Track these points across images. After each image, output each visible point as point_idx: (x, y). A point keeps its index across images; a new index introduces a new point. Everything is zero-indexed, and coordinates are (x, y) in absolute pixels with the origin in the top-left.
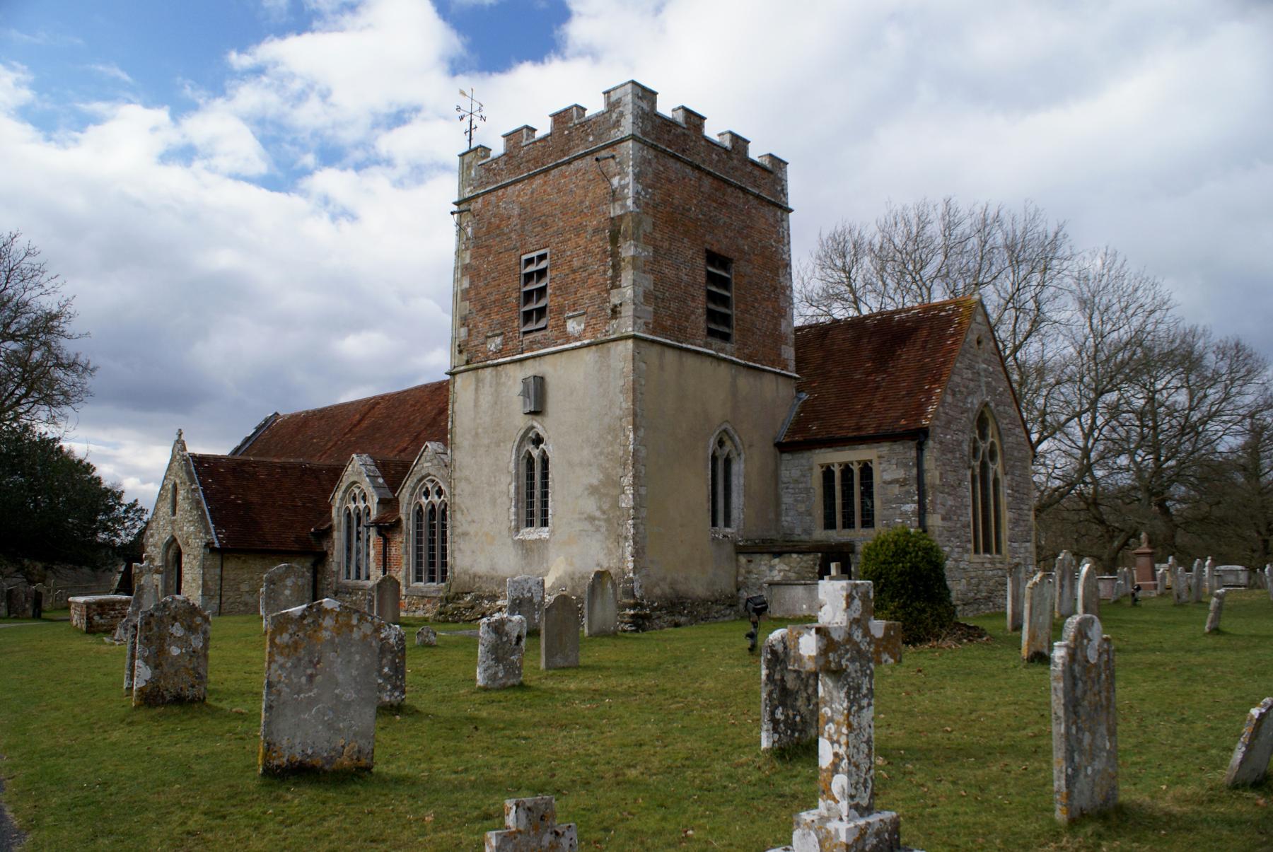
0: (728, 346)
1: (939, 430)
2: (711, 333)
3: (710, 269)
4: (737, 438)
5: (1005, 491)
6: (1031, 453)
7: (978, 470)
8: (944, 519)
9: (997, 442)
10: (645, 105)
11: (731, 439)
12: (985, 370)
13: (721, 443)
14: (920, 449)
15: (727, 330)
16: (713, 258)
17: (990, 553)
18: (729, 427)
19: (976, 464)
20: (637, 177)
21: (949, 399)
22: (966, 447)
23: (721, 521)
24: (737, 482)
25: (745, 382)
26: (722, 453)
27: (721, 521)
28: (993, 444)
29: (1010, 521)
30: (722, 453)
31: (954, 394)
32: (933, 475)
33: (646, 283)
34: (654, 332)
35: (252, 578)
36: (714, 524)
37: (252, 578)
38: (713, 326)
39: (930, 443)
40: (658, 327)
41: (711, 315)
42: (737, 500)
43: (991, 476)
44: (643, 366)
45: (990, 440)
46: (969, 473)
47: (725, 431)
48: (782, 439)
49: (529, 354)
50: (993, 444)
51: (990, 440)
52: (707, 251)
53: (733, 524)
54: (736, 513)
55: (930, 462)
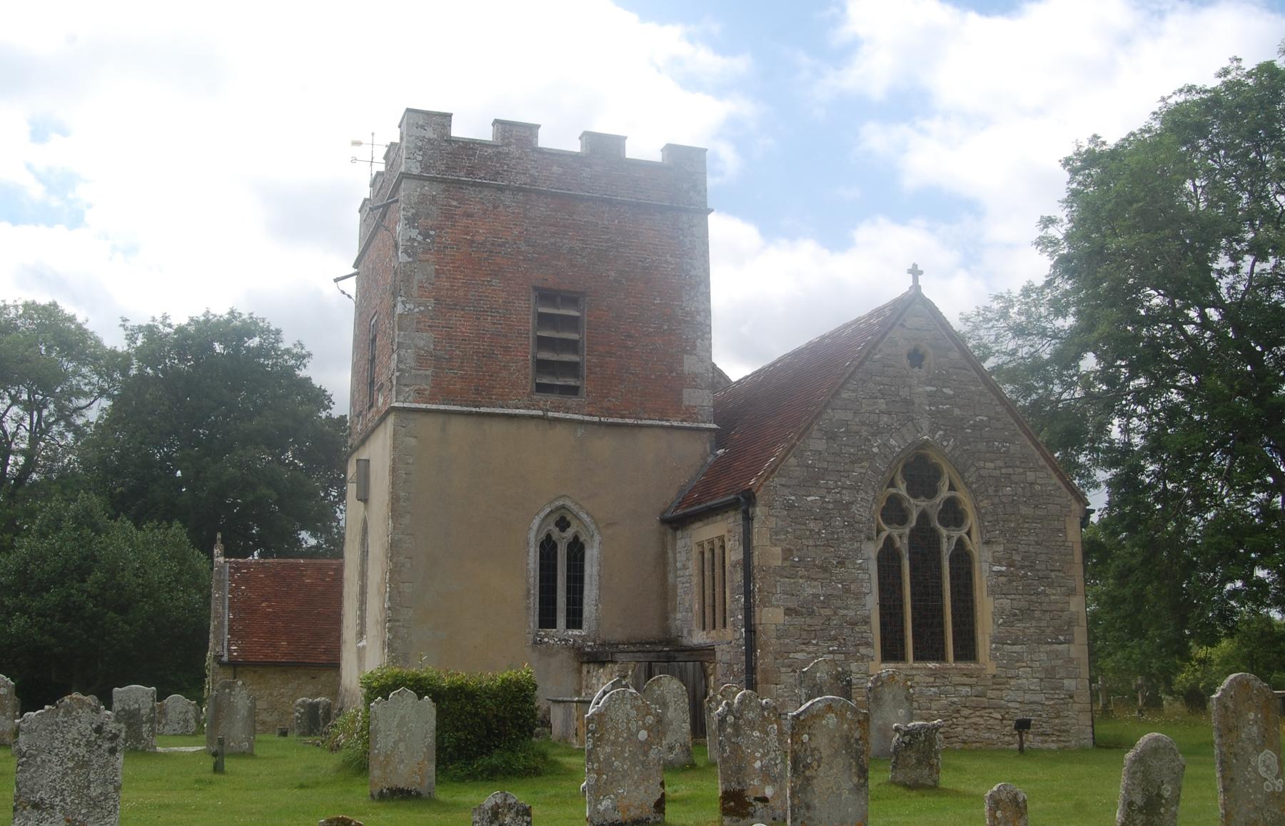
0: (571, 401)
1: (786, 491)
2: (541, 388)
3: (540, 310)
4: (584, 516)
5: (984, 571)
6: (1075, 506)
7: (902, 545)
8: (789, 611)
9: (963, 495)
10: (430, 134)
11: (576, 517)
12: (930, 395)
13: (563, 524)
14: (748, 519)
15: (571, 382)
16: (546, 295)
17: (941, 657)
18: (568, 503)
19: (901, 537)
20: (411, 222)
21: (821, 445)
22: (866, 508)
23: (561, 620)
24: (591, 570)
25: (604, 445)
26: (563, 541)
27: (561, 620)
28: (952, 504)
29: (999, 612)
30: (563, 541)
31: (831, 437)
32: (769, 553)
33: (422, 343)
34: (431, 399)
35: (271, 694)
36: (547, 619)
37: (271, 694)
38: (546, 380)
39: (759, 511)
40: (441, 391)
41: (542, 366)
42: (590, 592)
43: (946, 549)
44: (413, 441)
45: (944, 493)
46: (871, 550)
47: (563, 507)
48: (669, 515)
49: (561, 415)
50: (952, 504)
51: (944, 493)
52: (535, 289)
53: (585, 625)
54: (589, 609)
55: (760, 537)
